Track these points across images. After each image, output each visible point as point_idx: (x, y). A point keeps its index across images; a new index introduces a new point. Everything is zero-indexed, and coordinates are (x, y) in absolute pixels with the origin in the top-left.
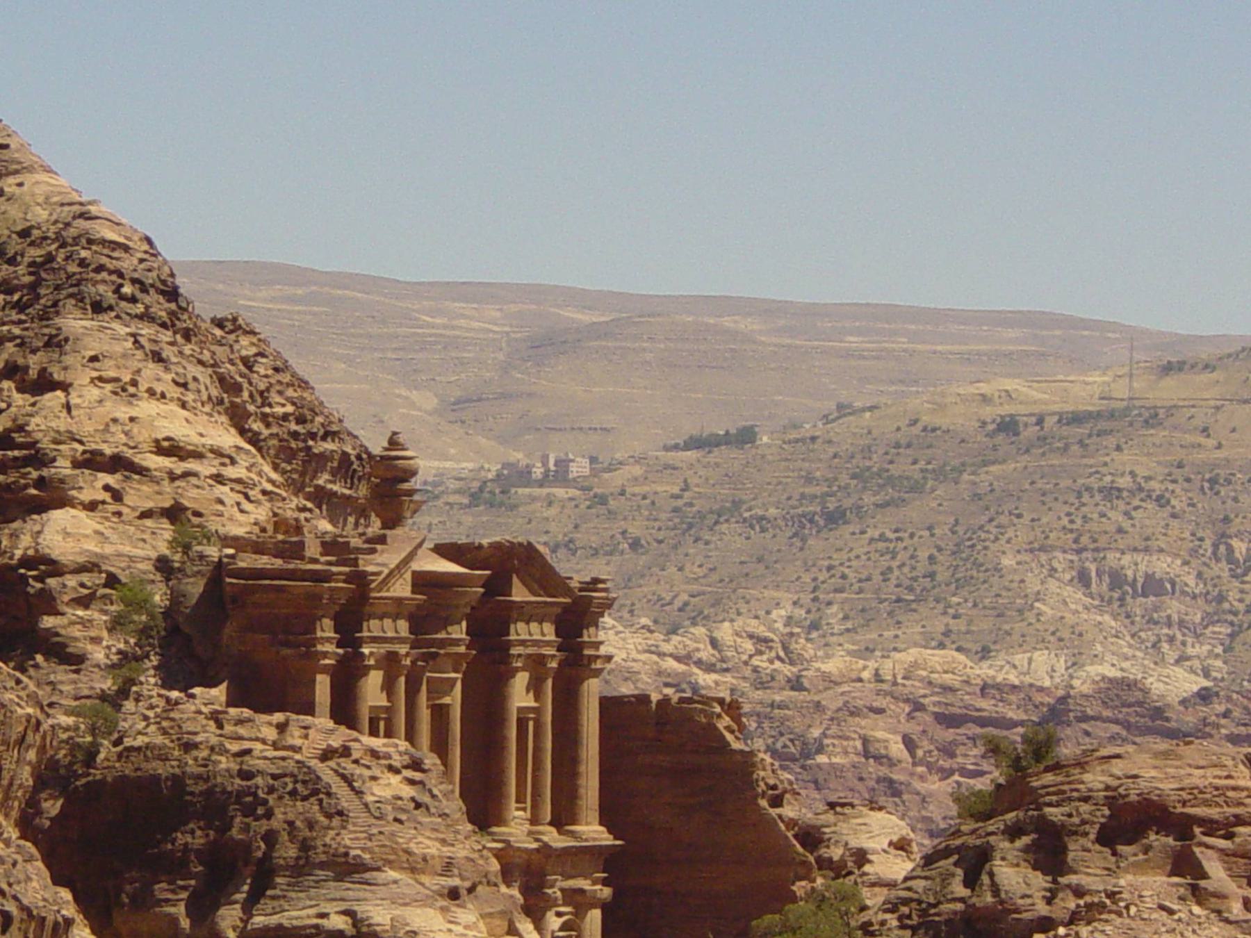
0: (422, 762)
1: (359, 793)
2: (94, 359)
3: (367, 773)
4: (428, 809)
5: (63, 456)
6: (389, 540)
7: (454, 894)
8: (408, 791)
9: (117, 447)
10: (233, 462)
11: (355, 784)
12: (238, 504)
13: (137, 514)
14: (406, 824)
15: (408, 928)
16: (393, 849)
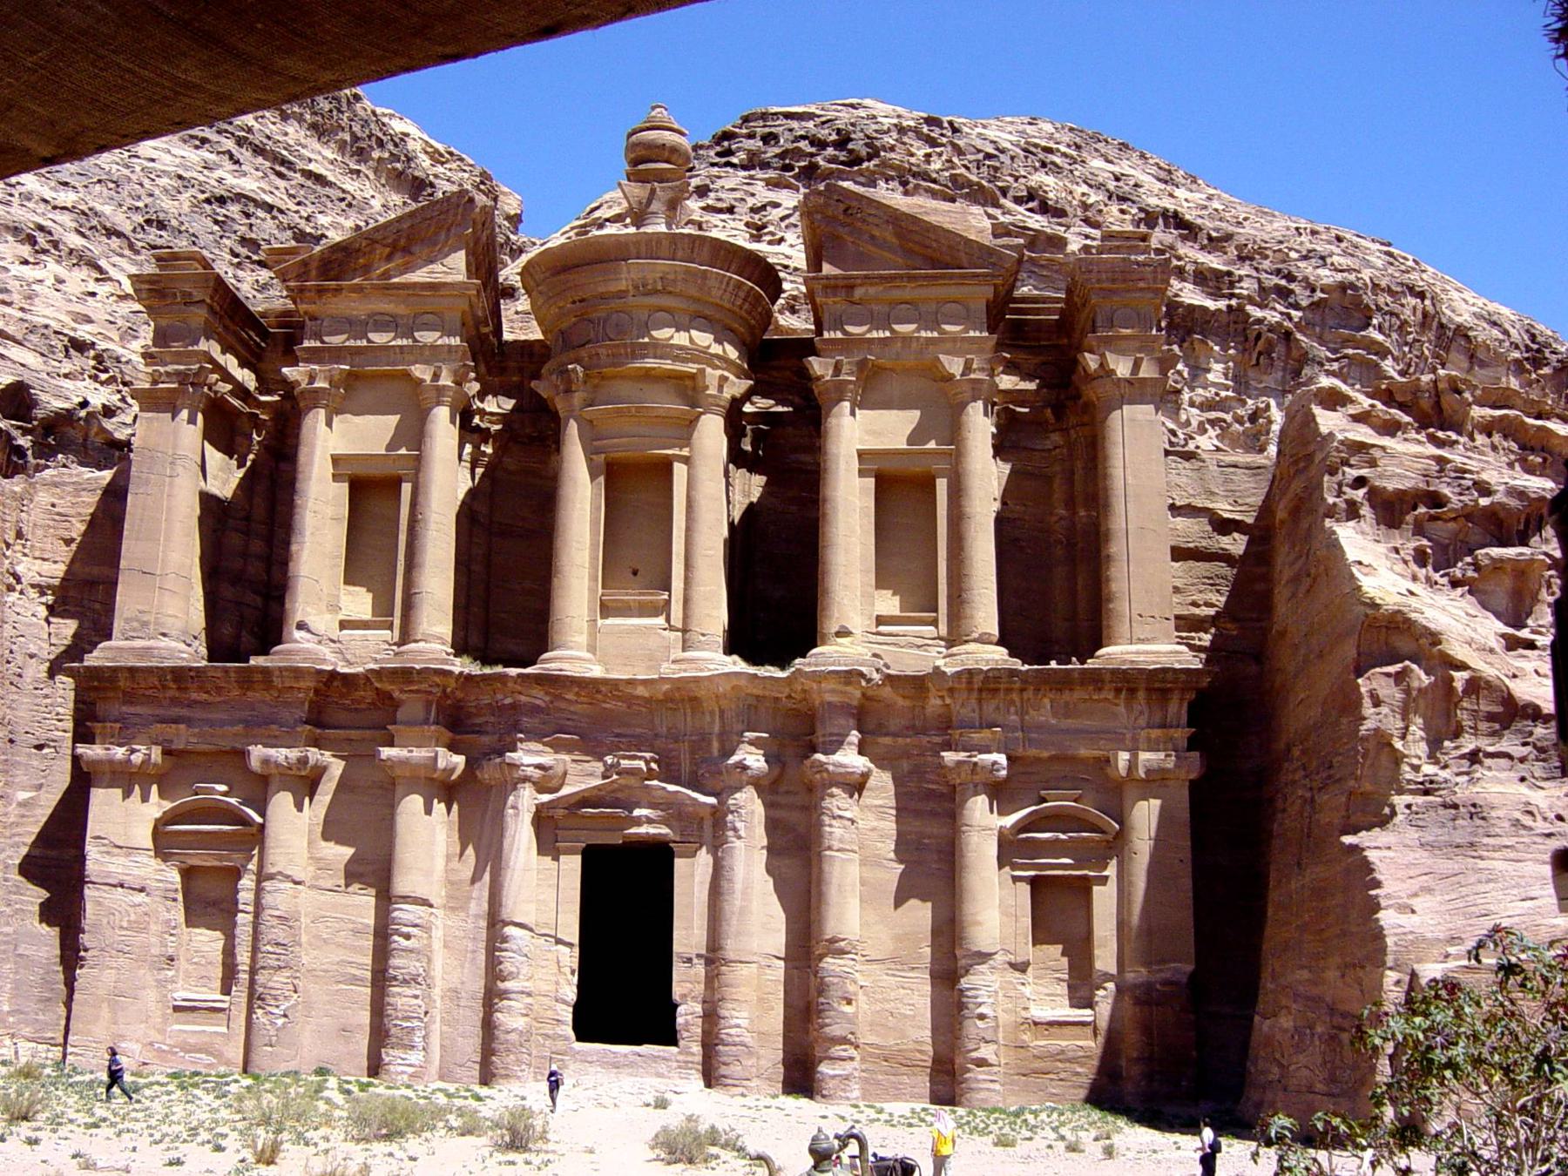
2: (597, 208)
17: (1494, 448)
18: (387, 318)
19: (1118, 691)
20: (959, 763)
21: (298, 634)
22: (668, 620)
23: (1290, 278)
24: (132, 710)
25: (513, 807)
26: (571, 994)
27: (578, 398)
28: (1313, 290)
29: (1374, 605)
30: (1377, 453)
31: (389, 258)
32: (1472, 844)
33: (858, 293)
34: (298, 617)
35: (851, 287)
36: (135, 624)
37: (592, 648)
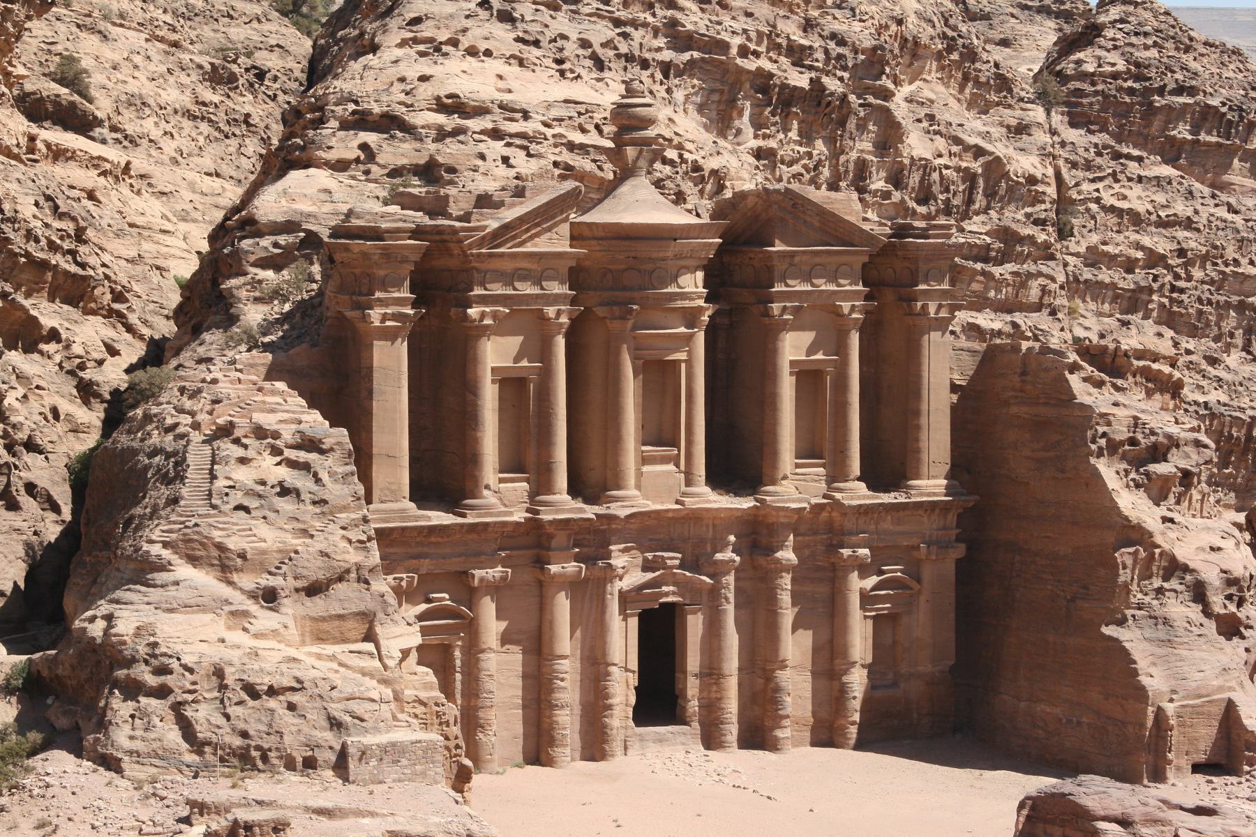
0: (320, 441)
1: (213, 477)
2: (417, 21)
3: (240, 452)
4: (298, 494)
5: (334, 117)
6: (527, 194)
7: (270, 597)
8: (284, 473)
9: (388, 106)
10: (526, 116)
11: (216, 467)
12: (505, 160)
13: (386, 171)
14: (254, 513)
15: (152, 639)
16: (202, 544)
17: (1136, 383)
18: (525, 272)
19: (926, 510)
20: (850, 556)
21: (486, 492)
22: (677, 465)
23: (842, 42)
24: (391, 550)
25: (610, 594)
26: (633, 700)
27: (630, 324)
28: (856, 53)
29: (1126, 518)
30: (1111, 418)
31: (527, 230)
32: (1169, 641)
33: (797, 259)
34: (485, 482)
35: (794, 256)
36: (386, 492)
37: (638, 487)
